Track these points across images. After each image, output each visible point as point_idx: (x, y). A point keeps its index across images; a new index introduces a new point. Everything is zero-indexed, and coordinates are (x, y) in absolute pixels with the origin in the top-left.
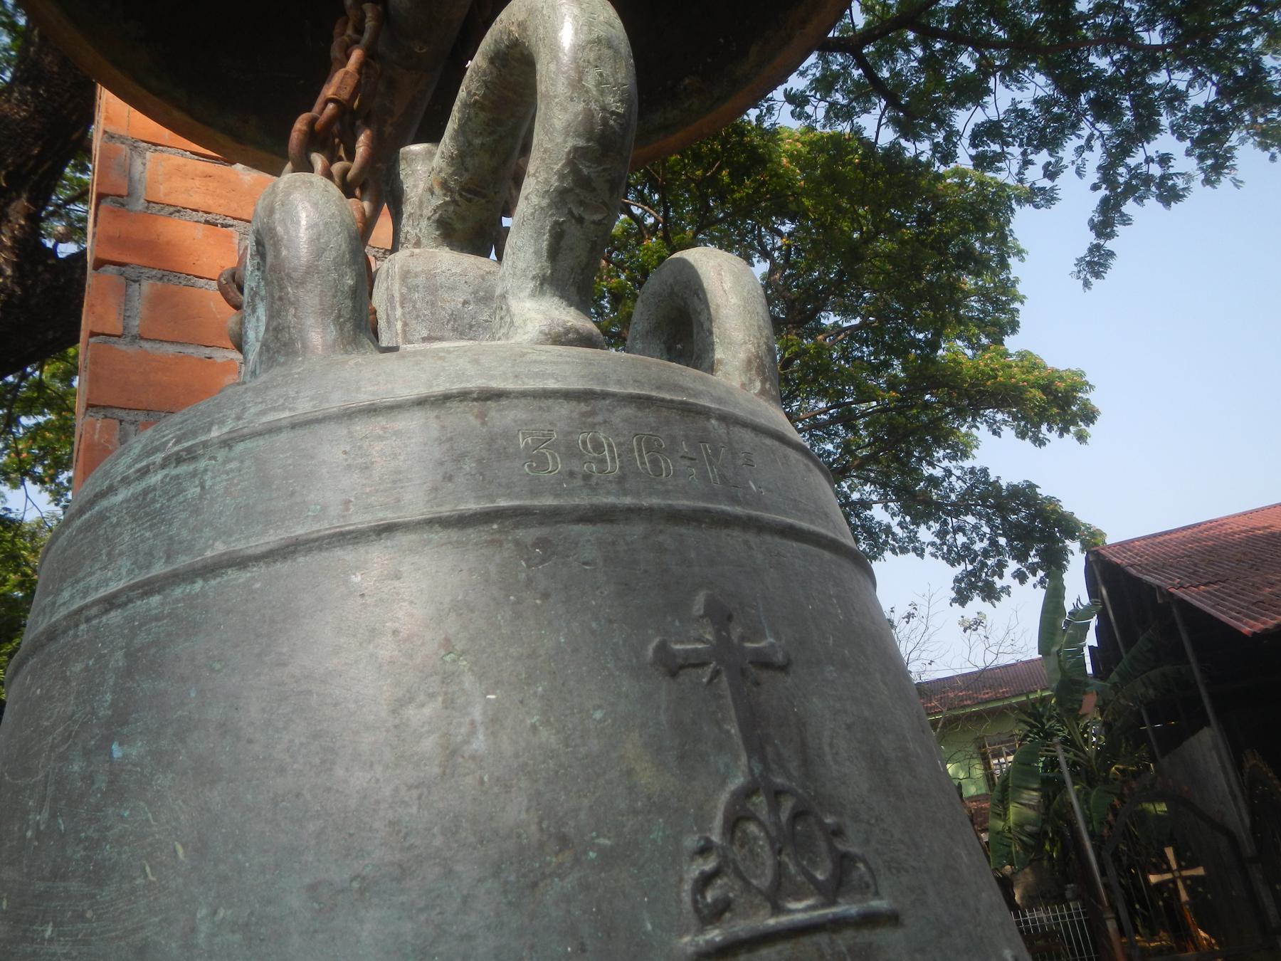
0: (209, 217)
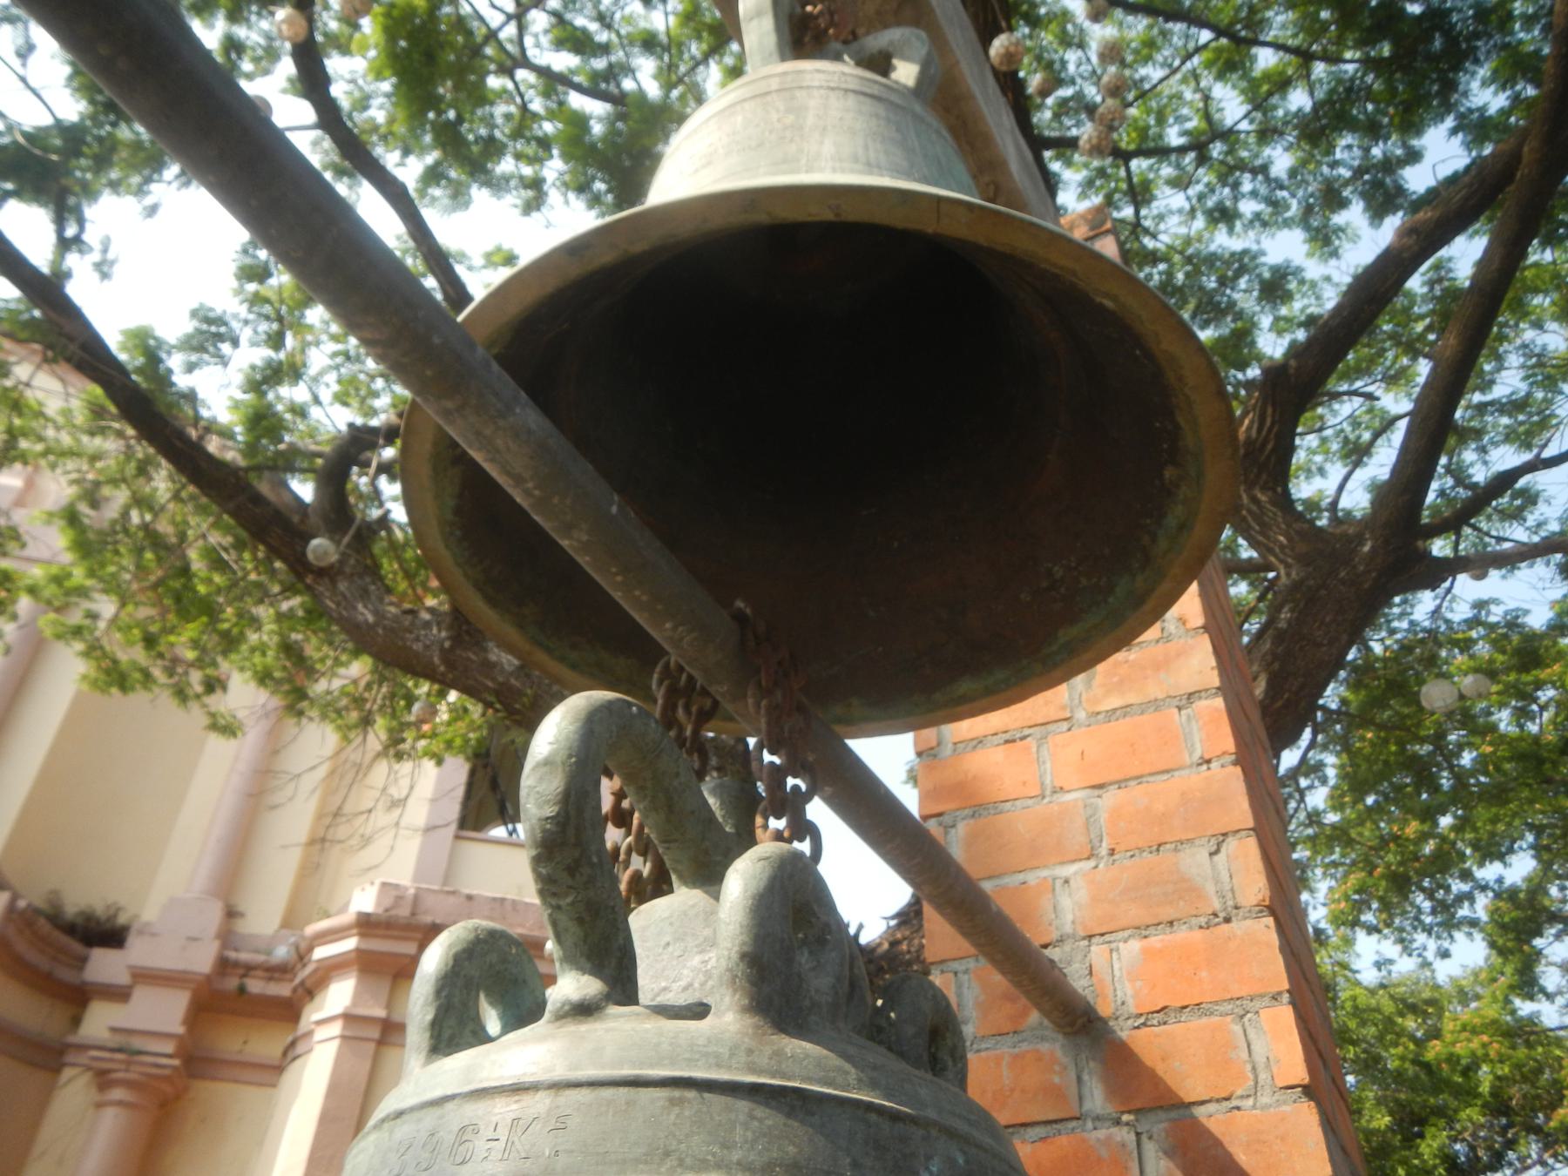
0: (1007, 736)
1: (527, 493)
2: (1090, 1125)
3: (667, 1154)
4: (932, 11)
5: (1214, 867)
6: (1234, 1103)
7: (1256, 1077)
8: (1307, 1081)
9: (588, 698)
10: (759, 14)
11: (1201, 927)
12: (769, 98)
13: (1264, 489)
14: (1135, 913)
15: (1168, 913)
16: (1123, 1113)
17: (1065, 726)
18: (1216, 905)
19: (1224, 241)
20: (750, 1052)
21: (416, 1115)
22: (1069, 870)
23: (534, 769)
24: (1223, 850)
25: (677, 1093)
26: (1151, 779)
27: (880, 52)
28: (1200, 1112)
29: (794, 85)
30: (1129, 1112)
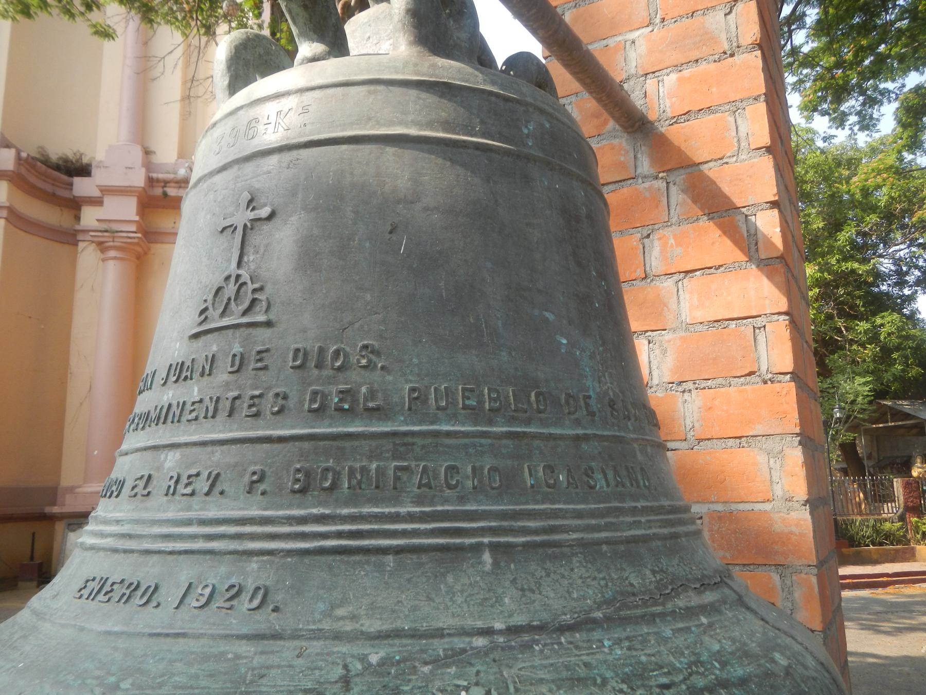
2: (640, 181)
3: (369, 119)
5: (727, 22)
6: (725, 160)
7: (739, 145)
8: (768, 144)
11: (715, 61)
16: (660, 172)
18: (726, 46)
20: (416, 65)
21: (223, 122)
24: (734, 11)
25: (372, 88)
28: (704, 168)
30: (663, 172)
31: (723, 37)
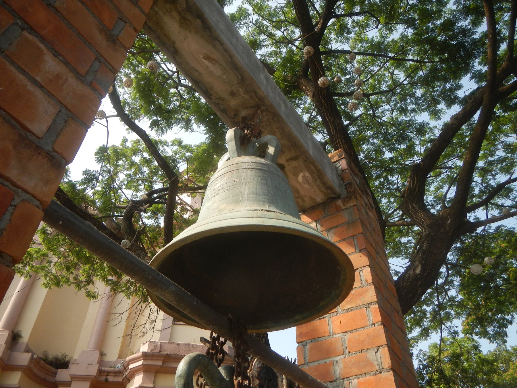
1: (174, 304)
4: (282, 118)
9: (190, 356)
10: (231, 141)
11: (373, 375)
12: (232, 173)
13: (416, 204)
14: (355, 371)
15: (365, 371)
17: (335, 314)
18: (377, 368)
19: (404, 118)
22: (338, 358)
23: (178, 377)
26: (359, 330)
27: (265, 142)
29: (239, 168)
31: (376, 363)
